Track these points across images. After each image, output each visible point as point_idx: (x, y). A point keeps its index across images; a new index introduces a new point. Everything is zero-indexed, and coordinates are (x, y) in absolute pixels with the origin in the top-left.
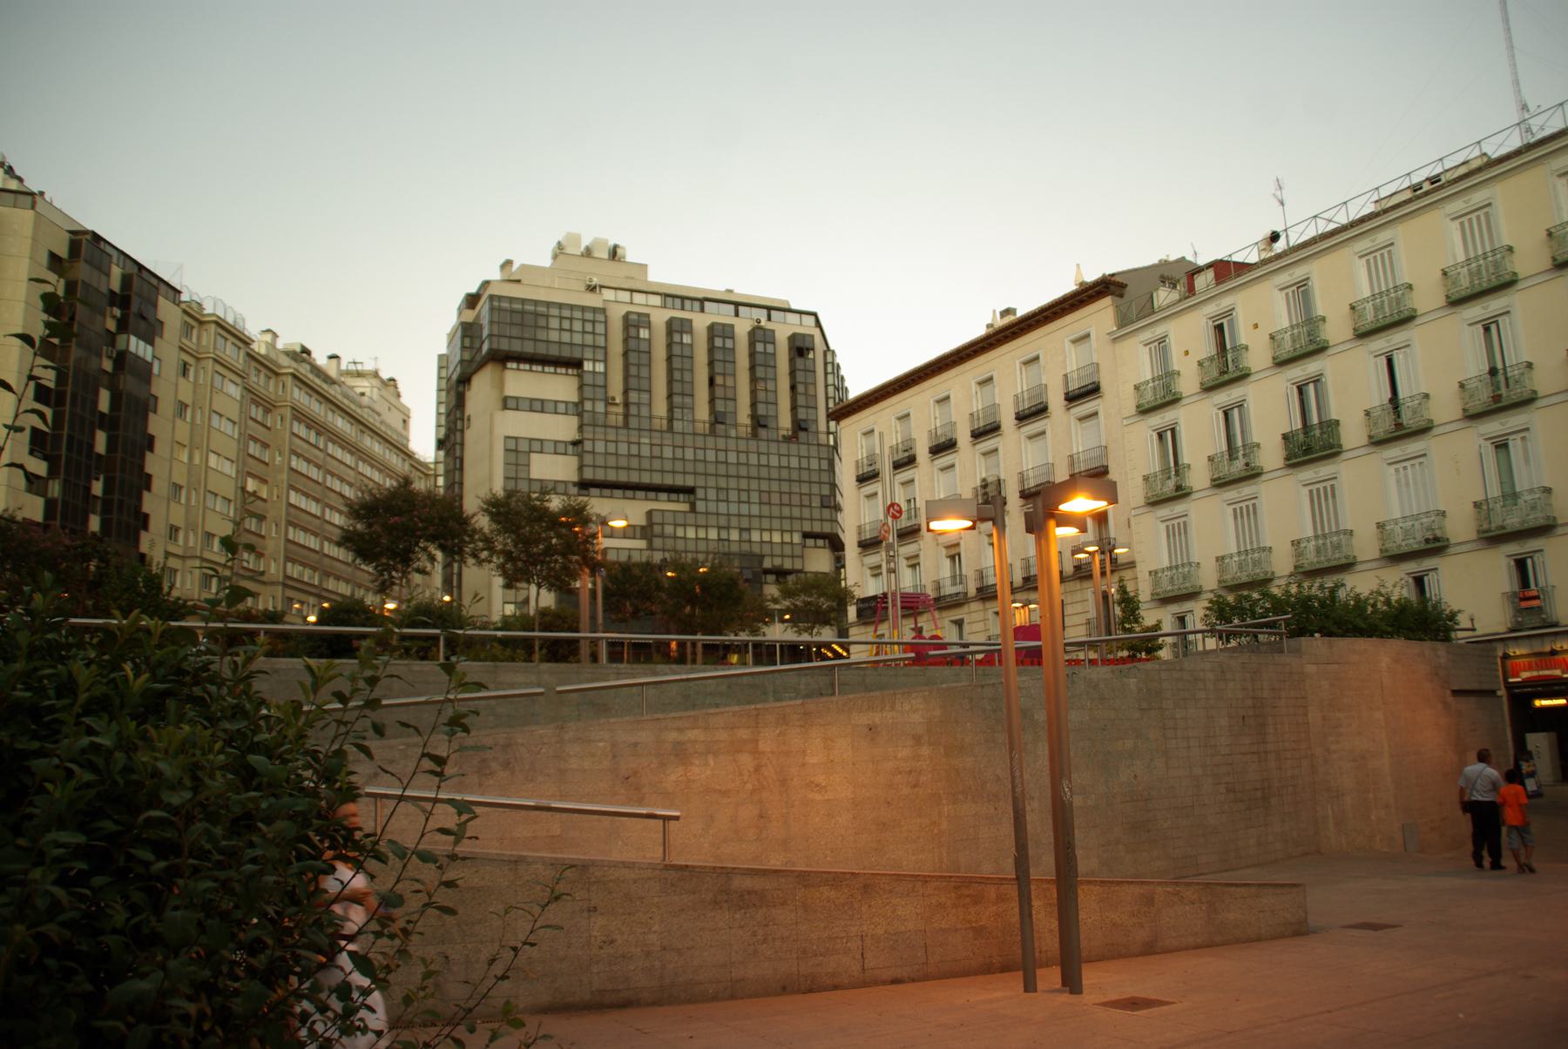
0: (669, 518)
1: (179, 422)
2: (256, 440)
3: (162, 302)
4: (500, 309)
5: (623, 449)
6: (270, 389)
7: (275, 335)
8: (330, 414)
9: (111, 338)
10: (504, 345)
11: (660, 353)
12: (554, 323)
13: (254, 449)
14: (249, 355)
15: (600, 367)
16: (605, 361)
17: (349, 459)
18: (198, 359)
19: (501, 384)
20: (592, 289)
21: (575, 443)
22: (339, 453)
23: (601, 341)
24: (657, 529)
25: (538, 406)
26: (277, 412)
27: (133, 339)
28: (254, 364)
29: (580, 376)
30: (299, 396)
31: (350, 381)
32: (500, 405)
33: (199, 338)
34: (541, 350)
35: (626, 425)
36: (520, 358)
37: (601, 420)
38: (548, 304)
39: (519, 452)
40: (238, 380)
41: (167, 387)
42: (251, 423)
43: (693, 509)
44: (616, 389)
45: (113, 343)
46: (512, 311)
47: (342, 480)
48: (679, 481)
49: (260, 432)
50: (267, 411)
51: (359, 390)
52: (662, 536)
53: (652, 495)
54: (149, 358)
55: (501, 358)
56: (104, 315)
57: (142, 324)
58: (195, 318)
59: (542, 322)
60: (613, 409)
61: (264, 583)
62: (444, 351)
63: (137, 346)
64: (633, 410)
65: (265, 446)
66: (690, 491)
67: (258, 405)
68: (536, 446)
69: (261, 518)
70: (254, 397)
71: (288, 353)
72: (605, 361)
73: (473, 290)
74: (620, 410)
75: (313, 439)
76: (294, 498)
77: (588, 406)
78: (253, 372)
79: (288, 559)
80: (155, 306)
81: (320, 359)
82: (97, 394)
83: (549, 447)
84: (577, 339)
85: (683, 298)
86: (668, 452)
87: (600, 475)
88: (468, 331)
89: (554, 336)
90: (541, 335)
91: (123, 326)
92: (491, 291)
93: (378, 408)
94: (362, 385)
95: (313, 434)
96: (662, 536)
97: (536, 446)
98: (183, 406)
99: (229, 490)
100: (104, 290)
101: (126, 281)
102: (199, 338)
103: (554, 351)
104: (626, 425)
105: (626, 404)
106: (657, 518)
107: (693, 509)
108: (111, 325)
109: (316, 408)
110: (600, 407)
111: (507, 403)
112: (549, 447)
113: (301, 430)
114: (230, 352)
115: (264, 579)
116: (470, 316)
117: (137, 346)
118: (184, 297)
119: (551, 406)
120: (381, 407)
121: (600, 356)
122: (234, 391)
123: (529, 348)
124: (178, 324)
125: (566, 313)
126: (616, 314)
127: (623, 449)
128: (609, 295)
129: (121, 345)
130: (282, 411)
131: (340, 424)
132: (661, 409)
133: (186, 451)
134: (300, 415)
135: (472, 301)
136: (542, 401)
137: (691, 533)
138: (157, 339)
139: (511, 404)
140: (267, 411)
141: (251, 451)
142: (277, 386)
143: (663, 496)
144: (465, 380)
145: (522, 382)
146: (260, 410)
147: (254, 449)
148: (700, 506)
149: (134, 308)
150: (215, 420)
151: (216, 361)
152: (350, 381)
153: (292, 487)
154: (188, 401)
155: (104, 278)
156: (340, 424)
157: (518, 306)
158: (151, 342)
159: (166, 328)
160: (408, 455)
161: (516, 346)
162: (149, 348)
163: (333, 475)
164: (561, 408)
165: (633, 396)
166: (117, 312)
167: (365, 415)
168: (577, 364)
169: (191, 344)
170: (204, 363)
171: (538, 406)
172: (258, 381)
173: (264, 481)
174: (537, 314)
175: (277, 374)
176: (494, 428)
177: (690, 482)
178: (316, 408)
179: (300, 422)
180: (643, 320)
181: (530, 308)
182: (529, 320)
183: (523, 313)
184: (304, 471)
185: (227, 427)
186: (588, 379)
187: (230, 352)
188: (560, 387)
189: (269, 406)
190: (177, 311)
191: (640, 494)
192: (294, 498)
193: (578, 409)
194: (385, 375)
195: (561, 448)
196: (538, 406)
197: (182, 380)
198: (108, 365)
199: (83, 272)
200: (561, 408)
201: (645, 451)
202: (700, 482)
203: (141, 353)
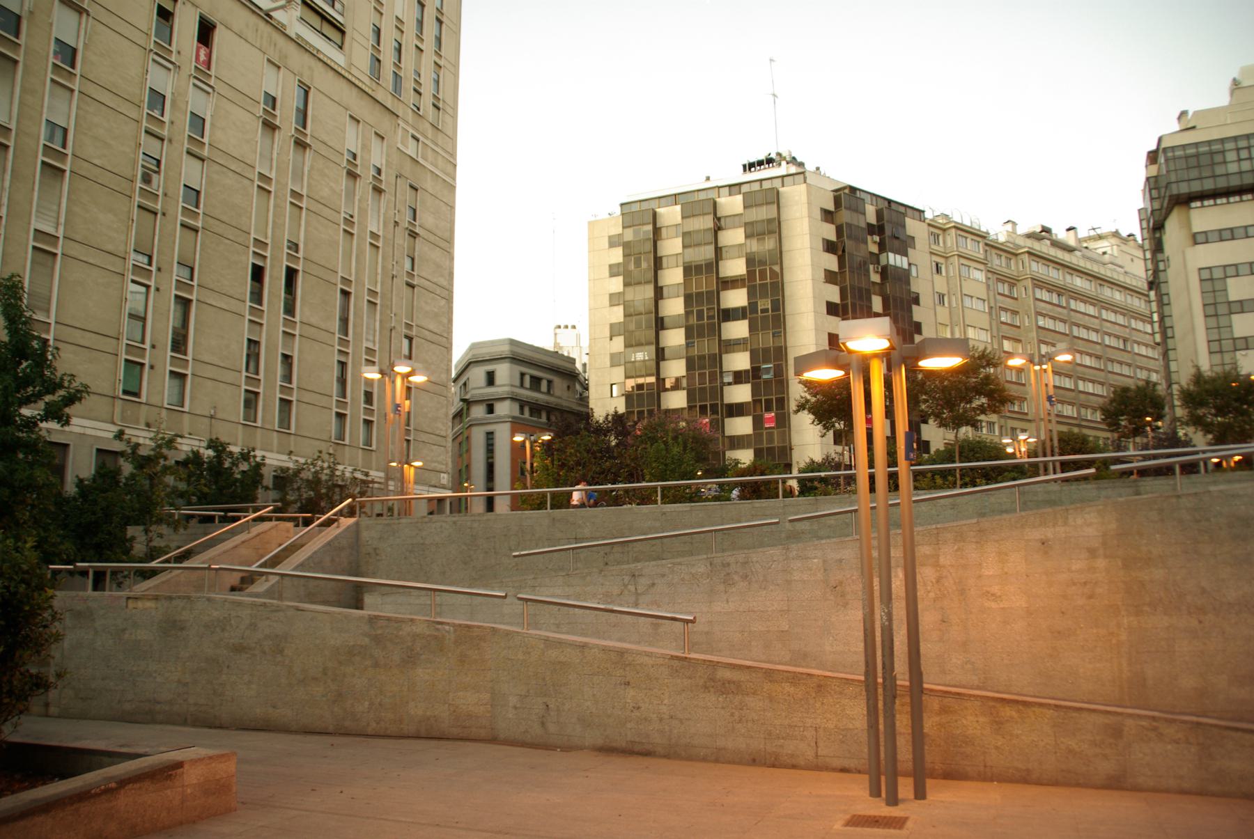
1: (939, 308)
2: (1006, 310)
3: (909, 222)
4: (1174, 158)
6: (1014, 268)
7: (1014, 224)
8: (1068, 277)
9: (877, 256)
10: (1184, 189)
14: (987, 245)
17: (1091, 310)
18: (947, 258)
19: (1188, 225)
22: (1081, 307)
26: (1020, 285)
27: (891, 255)
28: (994, 251)
30: (1037, 268)
31: (1092, 245)
32: (1191, 242)
33: (944, 242)
34: (1222, 183)
36: (1202, 196)
40: (982, 267)
41: (923, 283)
42: (999, 297)
45: (878, 263)
46: (1187, 157)
47: (1087, 328)
49: (1008, 303)
51: (1100, 251)
54: (906, 266)
55: (1184, 201)
56: (866, 243)
57: (896, 242)
58: (939, 229)
61: (1029, 421)
62: (1142, 206)
63: (894, 259)
65: (1015, 313)
67: (1003, 282)
71: (1030, 236)
73: (1154, 147)
75: (1055, 301)
78: (995, 257)
80: (904, 226)
82: (870, 300)
88: (1153, 184)
91: (882, 247)
93: (1119, 262)
94: (1103, 246)
95: (1055, 296)
98: (941, 296)
100: (863, 225)
101: (879, 214)
102: (944, 242)
108: (874, 249)
109: (1054, 275)
113: (1045, 295)
114: (973, 248)
115: (1029, 417)
116: (1154, 170)
117: (894, 259)
118: (928, 215)
119: (1242, 231)
122: (980, 276)
123: (1209, 185)
124: (926, 235)
129: (883, 261)
130: (1024, 283)
133: (948, 329)
134: (1039, 283)
135: (1153, 157)
136: (1231, 230)
138: (910, 251)
139: (1200, 238)
140: (1012, 285)
141: (1003, 319)
142: (1017, 263)
145: (1205, 217)
146: (1006, 285)
149: (888, 232)
150: (967, 302)
151: (959, 256)
152: (1092, 245)
153: (1041, 342)
154: (945, 292)
155: (861, 217)
158: (906, 255)
159: (916, 240)
161: (1196, 187)
162: (905, 259)
163: (1078, 325)
166: (877, 238)
169: (939, 248)
170: (951, 259)
171: (1227, 235)
172: (998, 262)
175: (1016, 255)
176: (1188, 261)
178: (1054, 275)
179: (1041, 288)
184: (1052, 327)
185: (979, 305)
187: (973, 248)
189: (1013, 282)
190: (924, 226)
194: (1124, 234)
197: (936, 277)
198: (875, 278)
199: (845, 216)
203: (899, 264)
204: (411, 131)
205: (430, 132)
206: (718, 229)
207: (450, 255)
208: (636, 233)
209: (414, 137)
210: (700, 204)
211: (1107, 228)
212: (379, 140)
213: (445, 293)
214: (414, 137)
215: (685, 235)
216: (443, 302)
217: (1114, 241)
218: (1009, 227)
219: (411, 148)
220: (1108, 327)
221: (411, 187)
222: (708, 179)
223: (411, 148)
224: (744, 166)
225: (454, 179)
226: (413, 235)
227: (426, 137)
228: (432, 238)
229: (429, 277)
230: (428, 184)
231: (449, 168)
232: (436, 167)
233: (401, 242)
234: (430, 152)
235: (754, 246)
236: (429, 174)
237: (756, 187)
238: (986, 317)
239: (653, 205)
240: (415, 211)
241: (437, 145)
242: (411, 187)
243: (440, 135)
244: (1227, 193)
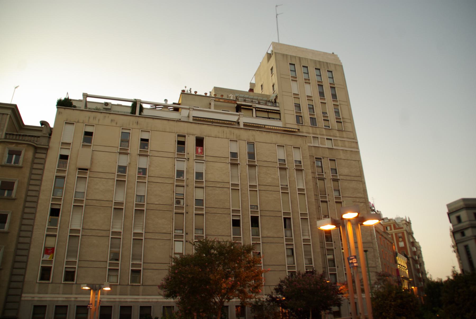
204: (326, 137)
205: (337, 134)
207: (364, 183)
209: (327, 139)
212: (297, 151)
213: (362, 200)
214: (327, 139)
216: (362, 204)
219: (328, 144)
221: (330, 160)
223: (328, 144)
225: (358, 148)
226: (337, 180)
227: (336, 137)
228: (348, 178)
229: (352, 196)
230: (342, 156)
231: (354, 145)
232: (345, 147)
233: (329, 185)
234: (339, 142)
236: (341, 151)
240: (336, 169)
241: (343, 137)
242: (330, 160)
243: (344, 133)
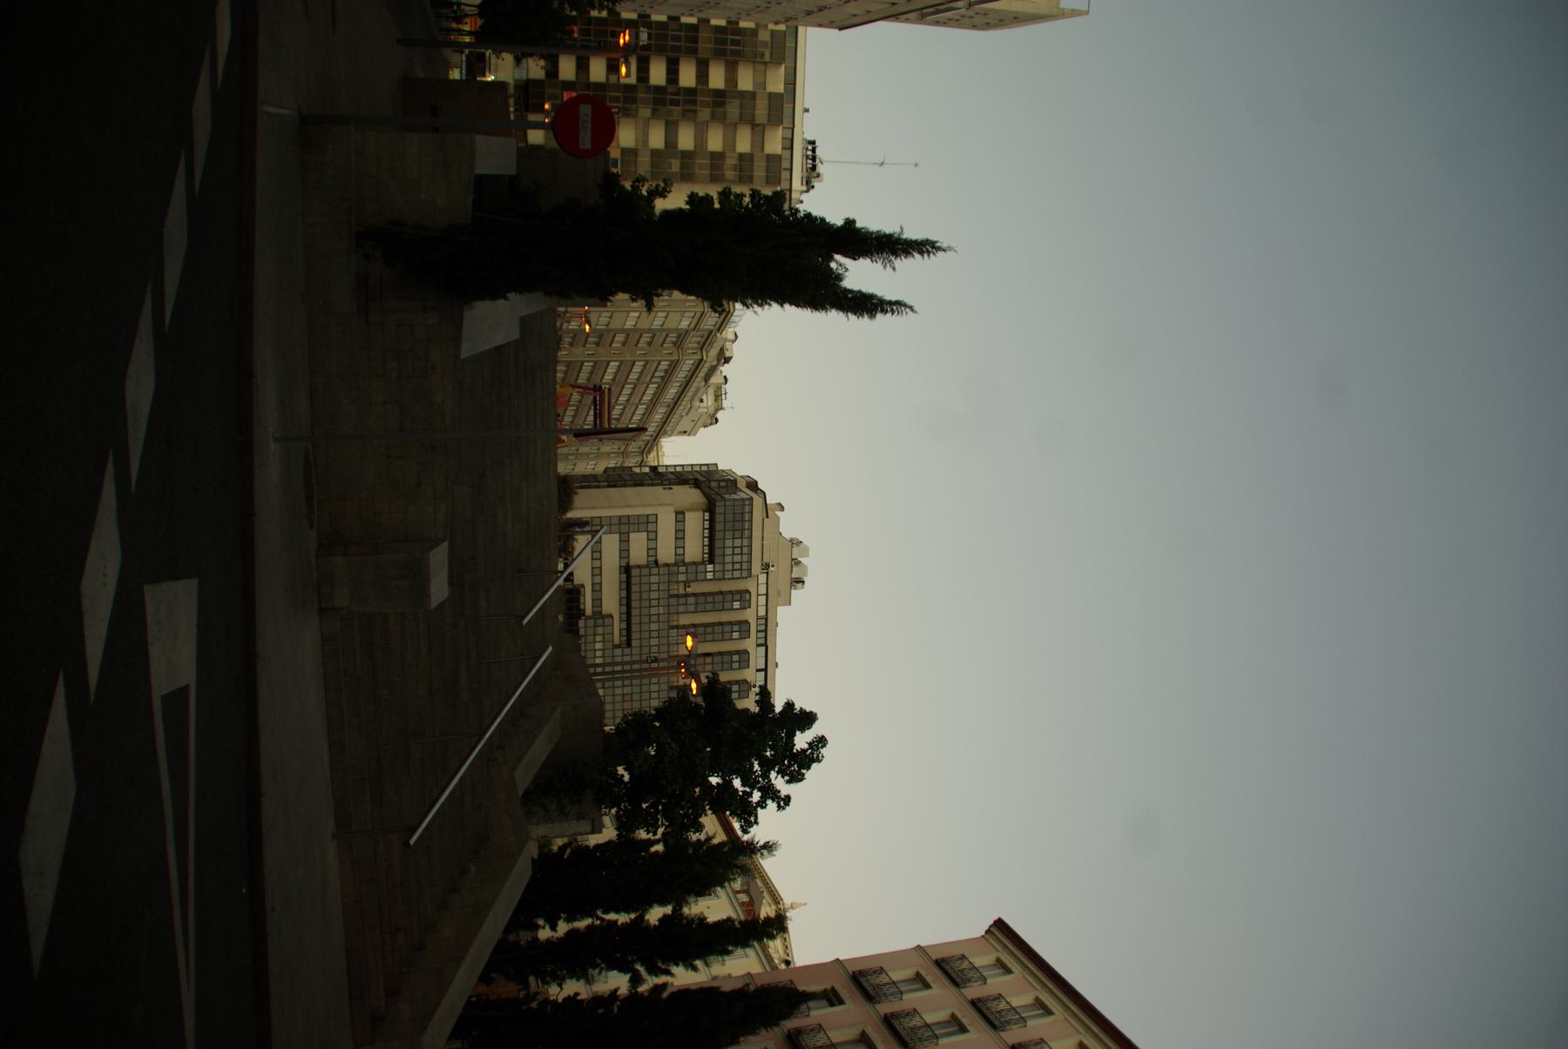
0: (608, 630)
5: (654, 595)
6: (692, 342)
10: (719, 510)
11: (725, 617)
12: (738, 542)
13: (646, 338)
15: (710, 576)
16: (714, 579)
17: (647, 398)
19: (692, 510)
20: (766, 567)
21: (656, 562)
22: (650, 391)
23: (728, 575)
24: (600, 622)
25: (680, 535)
29: (703, 562)
30: (688, 364)
31: (711, 391)
34: (718, 535)
35: (671, 596)
36: (712, 521)
37: (674, 578)
38: (750, 538)
39: (647, 524)
43: (615, 647)
44: (696, 588)
48: (635, 636)
50: (675, 344)
52: (595, 626)
53: (624, 617)
55: (710, 508)
59: (738, 534)
60: (681, 586)
64: (682, 601)
65: (650, 344)
66: (629, 644)
68: (652, 536)
69: (597, 344)
70: (682, 336)
71: (722, 350)
72: (714, 579)
74: (682, 591)
76: (614, 365)
77: (682, 569)
79: (569, 364)
81: (726, 369)
83: (652, 544)
84: (729, 559)
85: (766, 631)
86: (654, 626)
87: (634, 580)
89: (729, 543)
90: (729, 535)
92: (757, 500)
94: (709, 400)
96: (595, 626)
97: (652, 536)
99: (615, 325)
103: (718, 544)
104: (671, 596)
105: (686, 595)
106: (608, 621)
107: (615, 647)
109: (681, 375)
110: (682, 578)
111: (680, 514)
112: (652, 544)
113: (664, 365)
116: (742, 485)
120: (693, 414)
121: (718, 575)
122: (685, 324)
123: (719, 526)
125: (745, 550)
126: (749, 585)
127: (654, 595)
128: (762, 578)
131: (672, 391)
132: (685, 620)
134: (674, 365)
135: (753, 485)
137: (598, 646)
140: (675, 344)
143: (624, 625)
144: (697, 484)
145: (695, 523)
147: (646, 338)
148: (618, 652)
152: (711, 391)
153: (621, 363)
156: (672, 391)
157: (747, 517)
160: (661, 431)
161: (719, 518)
164: (680, 551)
165: (691, 600)
167: (685, 402)
168: (711, 561)
171: (680, 535)
173: (624, 344)
174: (742, 530)
176: (662, 505)
177: (635, 643)
178: (681, 375)
180: (746, 604)
181: (747, 525)
182: (738, 526)
183: (743, 521)
186: (701, 568)
188: (694, 549)
189: (678, 344)
191: (624, 609)
192: (614, 365)
193: (680, 562)
194: (719, 415)
195: (652, 552)
196: (680, 535)
200: (680, 551)
201: (654, 611)
202: (635, 651)
206: (754, 126)
208: (765, 44)
210: (782, 108)
211: (725, 404)
215: (753, 95)
217: (712, 410)
218: (732, 337)
220: (631, 409)
222: (807, 110)
224: (813, 143)
235: (731, 161)
237: (785, 164)
238: (647, 326)
239: (789, 60)
244: (711, 538)
